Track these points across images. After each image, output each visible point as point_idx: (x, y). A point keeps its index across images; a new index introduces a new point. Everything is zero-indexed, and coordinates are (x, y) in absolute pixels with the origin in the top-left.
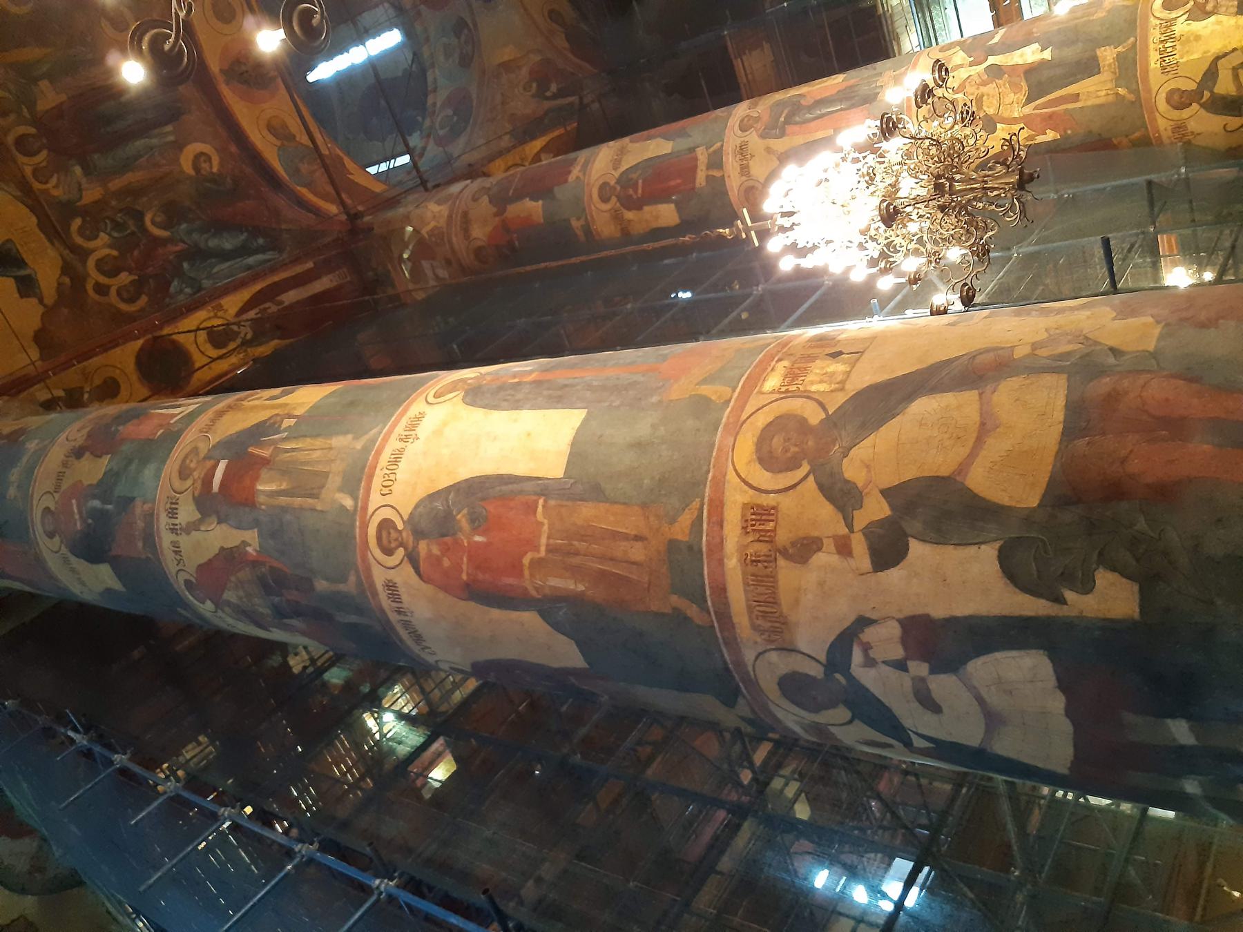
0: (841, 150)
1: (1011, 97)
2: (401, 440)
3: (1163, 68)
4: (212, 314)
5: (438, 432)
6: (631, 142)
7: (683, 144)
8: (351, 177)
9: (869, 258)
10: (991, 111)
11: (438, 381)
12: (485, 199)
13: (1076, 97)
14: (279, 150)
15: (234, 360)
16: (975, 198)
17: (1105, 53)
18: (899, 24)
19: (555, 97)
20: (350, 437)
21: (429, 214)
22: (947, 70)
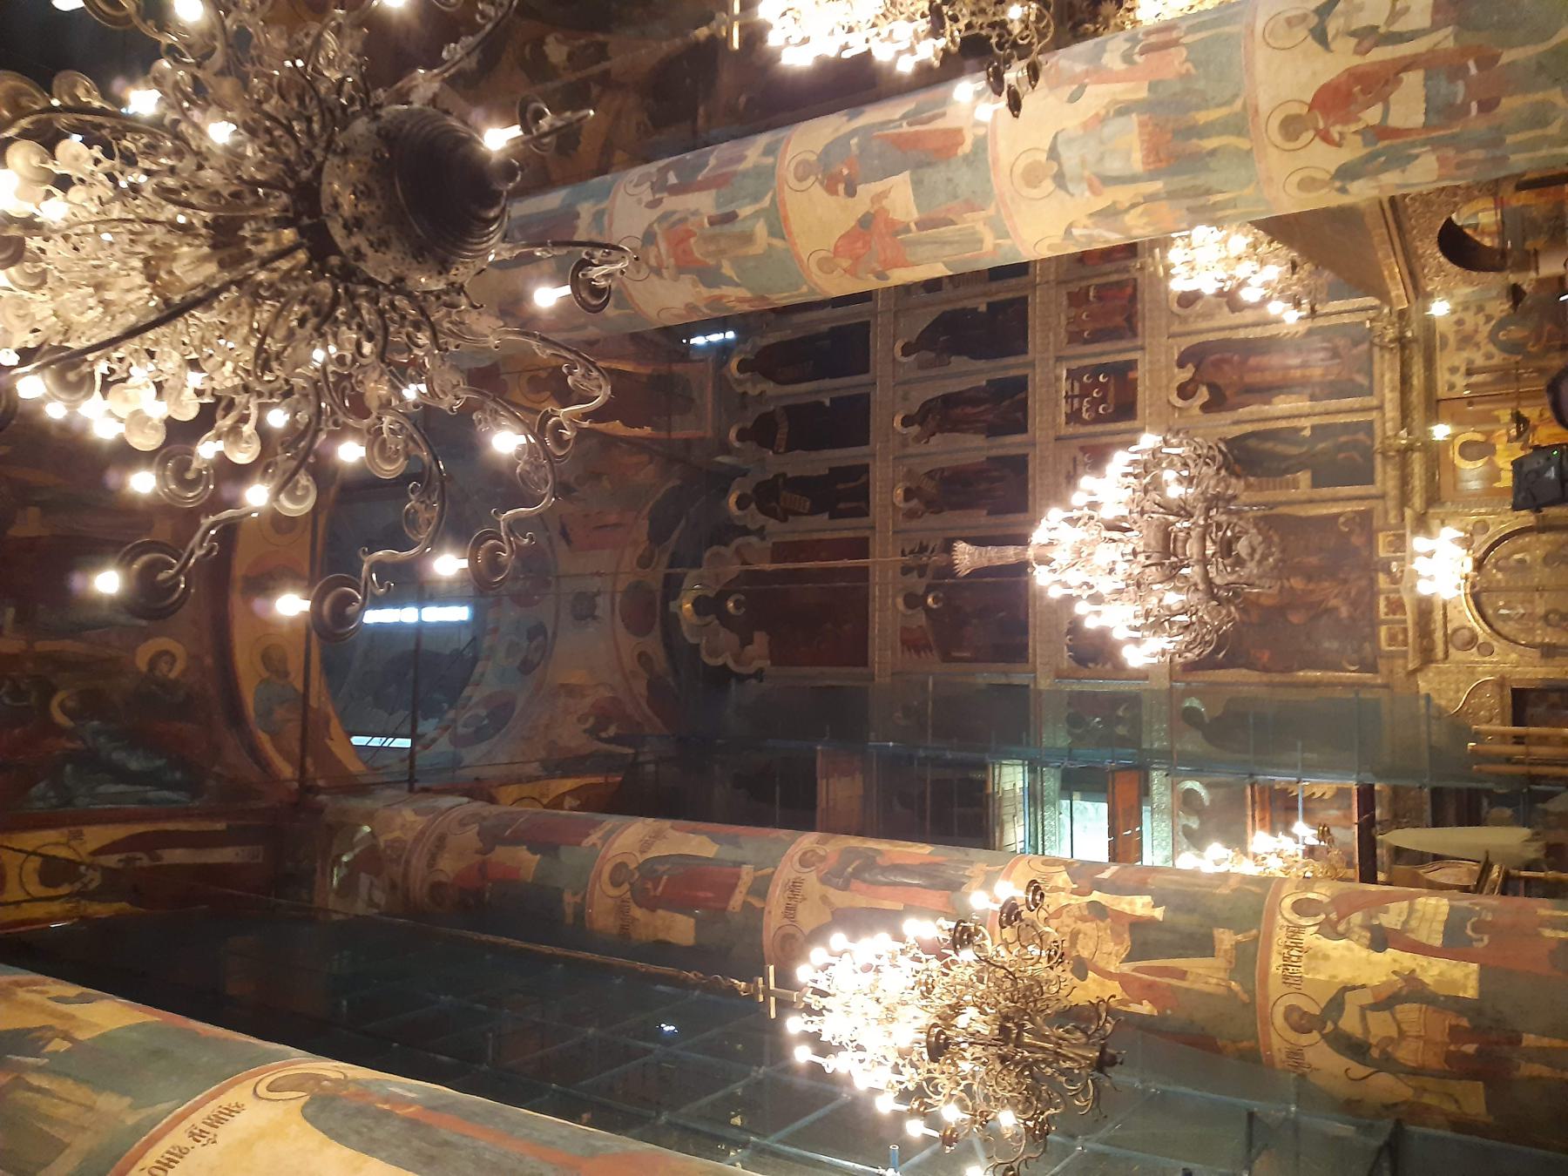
0: (903, 941)
1: (1110, 946)
2: (192, 1135)
3: (1286, 977)
4: (63, 840)
5: (247, 1145)
6: (672, 827)
7: (730, 853)
8: (329, 742)
9: (902, 1087)
10: (1085, 954)
11: (284, 1066)
12: (475, 828)
13: (1183, 975)
14: (261, 682)
15: (56, 907)
16: (1044, 1061)
18: (1007, 810)
19: (608, 741)
20: (127, 1101)
21: (399, 821)
22: (1042, 896)
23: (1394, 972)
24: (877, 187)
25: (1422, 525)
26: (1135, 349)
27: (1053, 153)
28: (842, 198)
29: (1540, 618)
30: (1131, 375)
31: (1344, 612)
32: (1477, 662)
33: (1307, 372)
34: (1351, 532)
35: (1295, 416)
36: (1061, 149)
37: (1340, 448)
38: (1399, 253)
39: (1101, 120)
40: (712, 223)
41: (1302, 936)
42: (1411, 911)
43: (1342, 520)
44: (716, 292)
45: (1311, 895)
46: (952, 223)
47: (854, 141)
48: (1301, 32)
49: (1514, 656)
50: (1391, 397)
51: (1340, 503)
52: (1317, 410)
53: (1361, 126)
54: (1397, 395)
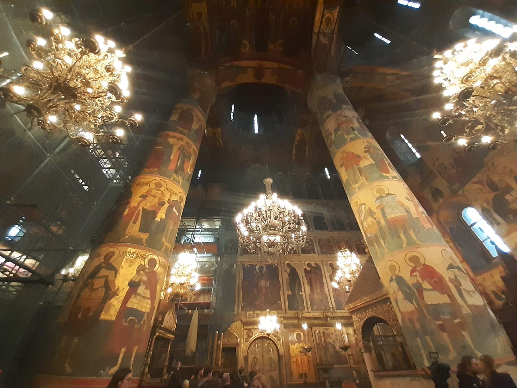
1: (149, 204)
13: (134, 222)
17: (146, 235)
23: (118, 288)
24: (369, 157)
25: (280, 322)
27: (388, 195)
28: (364, 150)
30: (312, 253)
31: (257, 302)
32: (243, 337)
33: (316, 294)
34: (277, 304)
35: (305, 290)
36: (390, 196)
37: (298, 302)
39: (402, 205)
40: (351, 127)
41: (141, 259)
42: (145, 298)
44: (333, 133)
45: (157, 266)
46: (361, 175)
47: (380, 152)
48: (450, 262)
49: (245, 348)
50: (311, 315)
51: (284, 302)
52: (307, 297)
53: (421, 282)
54: (312, 316)
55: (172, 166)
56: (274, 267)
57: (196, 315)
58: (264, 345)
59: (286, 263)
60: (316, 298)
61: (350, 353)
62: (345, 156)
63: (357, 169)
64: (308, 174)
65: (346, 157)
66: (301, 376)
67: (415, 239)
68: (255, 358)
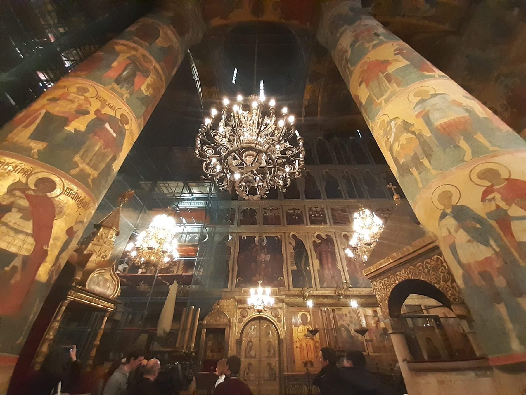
13: (26, 127)
26: (330, 224)
29: (251, 339)
30: (323, 223)
32: (236, 318)
38: (396, 263)
39: (460, 105)
43: (282, 278)
46: (389, 82)
49: (237, 330)
50: (321, 293)
51: (287, 278)
55: (112, 74)
56: (277, 239)
57: (173, 288)
58: (262, 327)
59: (291, 235)
60: (326, 274)
61: (368, 338)
62: (365, 68)
63: (384, 78)
64: (320, 137)
65: (368, 69)
66: (306, 364)
67: (487, 144)
68: (250, 341)
